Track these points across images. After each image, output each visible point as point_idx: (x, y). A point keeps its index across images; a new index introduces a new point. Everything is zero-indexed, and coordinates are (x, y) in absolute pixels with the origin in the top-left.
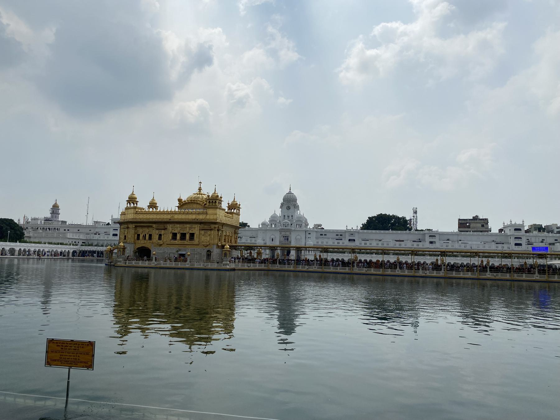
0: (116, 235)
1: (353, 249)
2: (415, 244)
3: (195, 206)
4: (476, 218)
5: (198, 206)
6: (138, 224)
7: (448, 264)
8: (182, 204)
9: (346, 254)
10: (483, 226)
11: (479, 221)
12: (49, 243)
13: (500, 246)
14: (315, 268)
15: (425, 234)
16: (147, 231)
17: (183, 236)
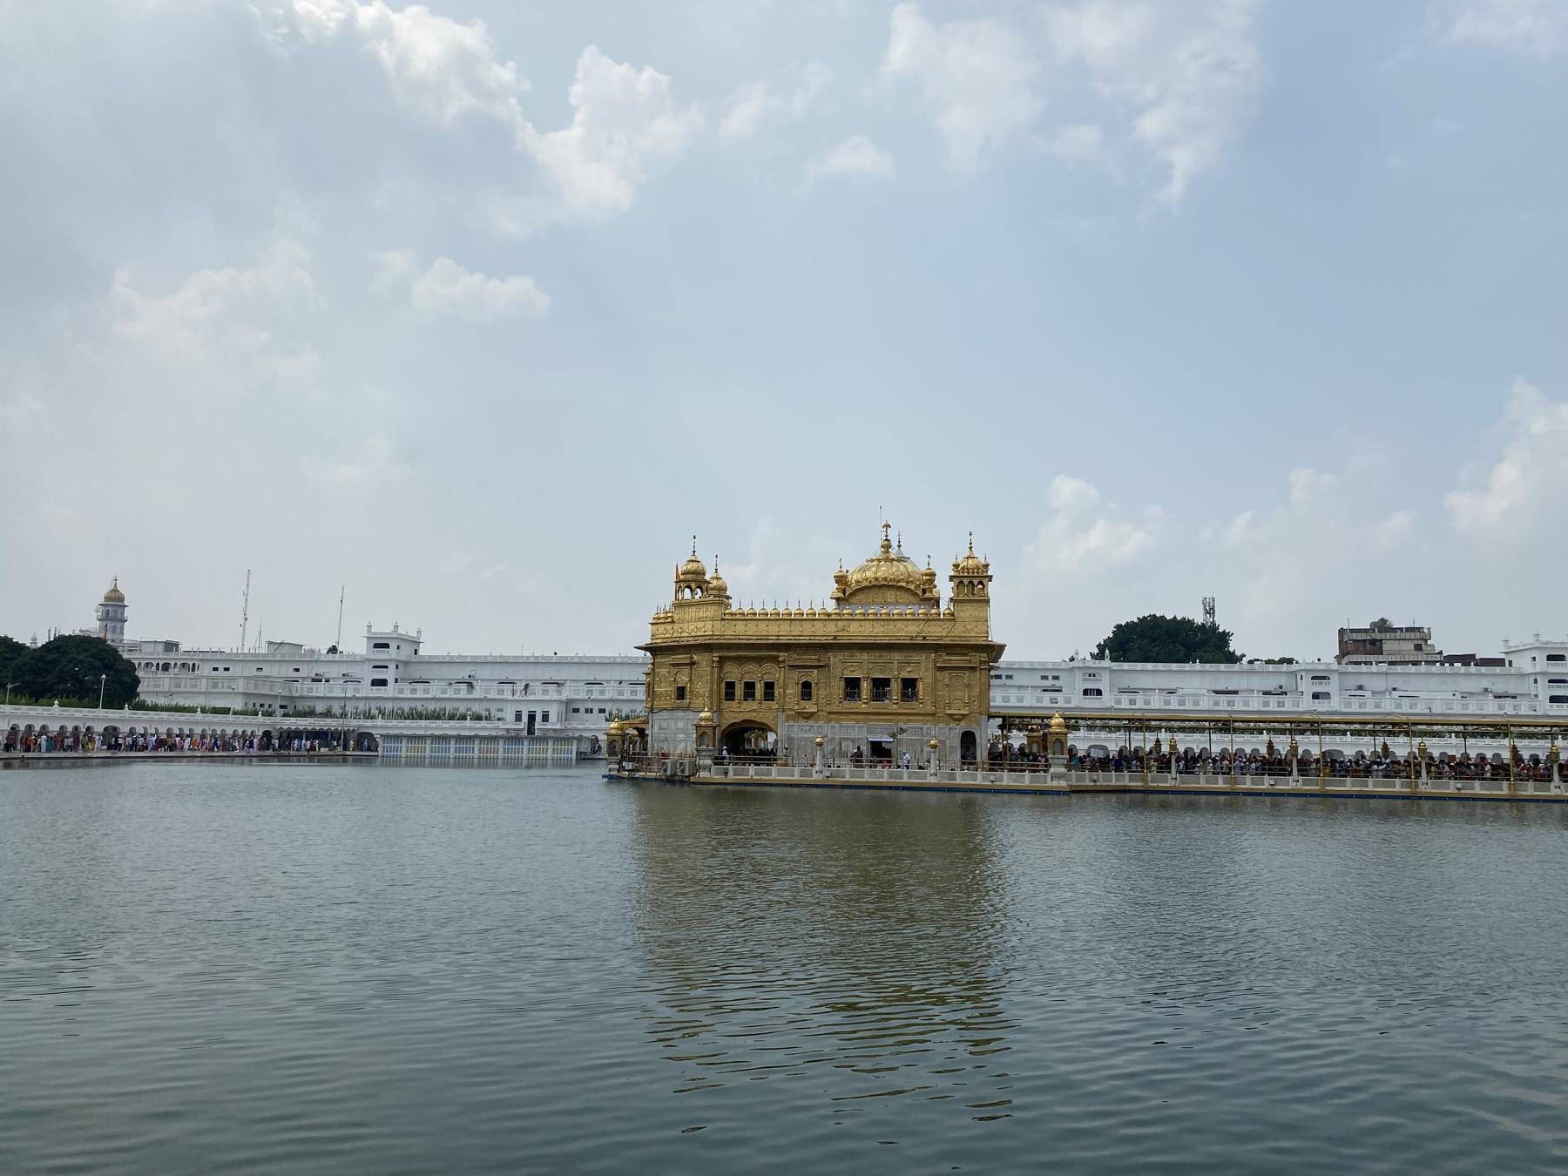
0: (383, 683)
1: (1226, 722)
2: (1273, 700)
3: (891, 596)
4: (1382, 626)
5: (903, 596)
6: (726, 652)
7: (1186, 752)
8: (848, 592)
9: (1082, 733)
10: (1418, 648)
11: (1408, 635)
12: (203, 711)
13: (1509, 703)
14: (1293, 783)
15: (1294, 673)
16: (757, 674)
17: (880, 686)
